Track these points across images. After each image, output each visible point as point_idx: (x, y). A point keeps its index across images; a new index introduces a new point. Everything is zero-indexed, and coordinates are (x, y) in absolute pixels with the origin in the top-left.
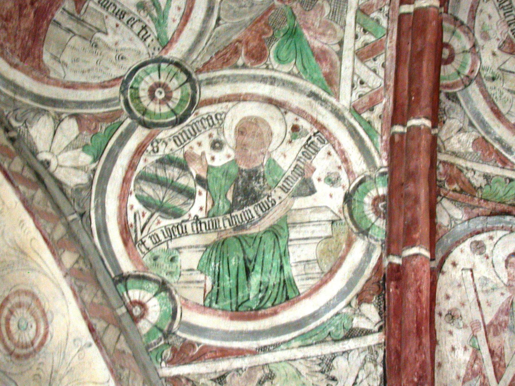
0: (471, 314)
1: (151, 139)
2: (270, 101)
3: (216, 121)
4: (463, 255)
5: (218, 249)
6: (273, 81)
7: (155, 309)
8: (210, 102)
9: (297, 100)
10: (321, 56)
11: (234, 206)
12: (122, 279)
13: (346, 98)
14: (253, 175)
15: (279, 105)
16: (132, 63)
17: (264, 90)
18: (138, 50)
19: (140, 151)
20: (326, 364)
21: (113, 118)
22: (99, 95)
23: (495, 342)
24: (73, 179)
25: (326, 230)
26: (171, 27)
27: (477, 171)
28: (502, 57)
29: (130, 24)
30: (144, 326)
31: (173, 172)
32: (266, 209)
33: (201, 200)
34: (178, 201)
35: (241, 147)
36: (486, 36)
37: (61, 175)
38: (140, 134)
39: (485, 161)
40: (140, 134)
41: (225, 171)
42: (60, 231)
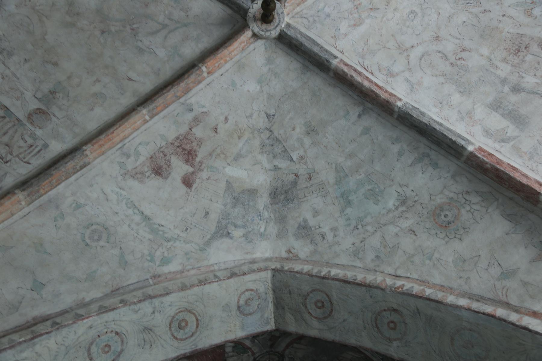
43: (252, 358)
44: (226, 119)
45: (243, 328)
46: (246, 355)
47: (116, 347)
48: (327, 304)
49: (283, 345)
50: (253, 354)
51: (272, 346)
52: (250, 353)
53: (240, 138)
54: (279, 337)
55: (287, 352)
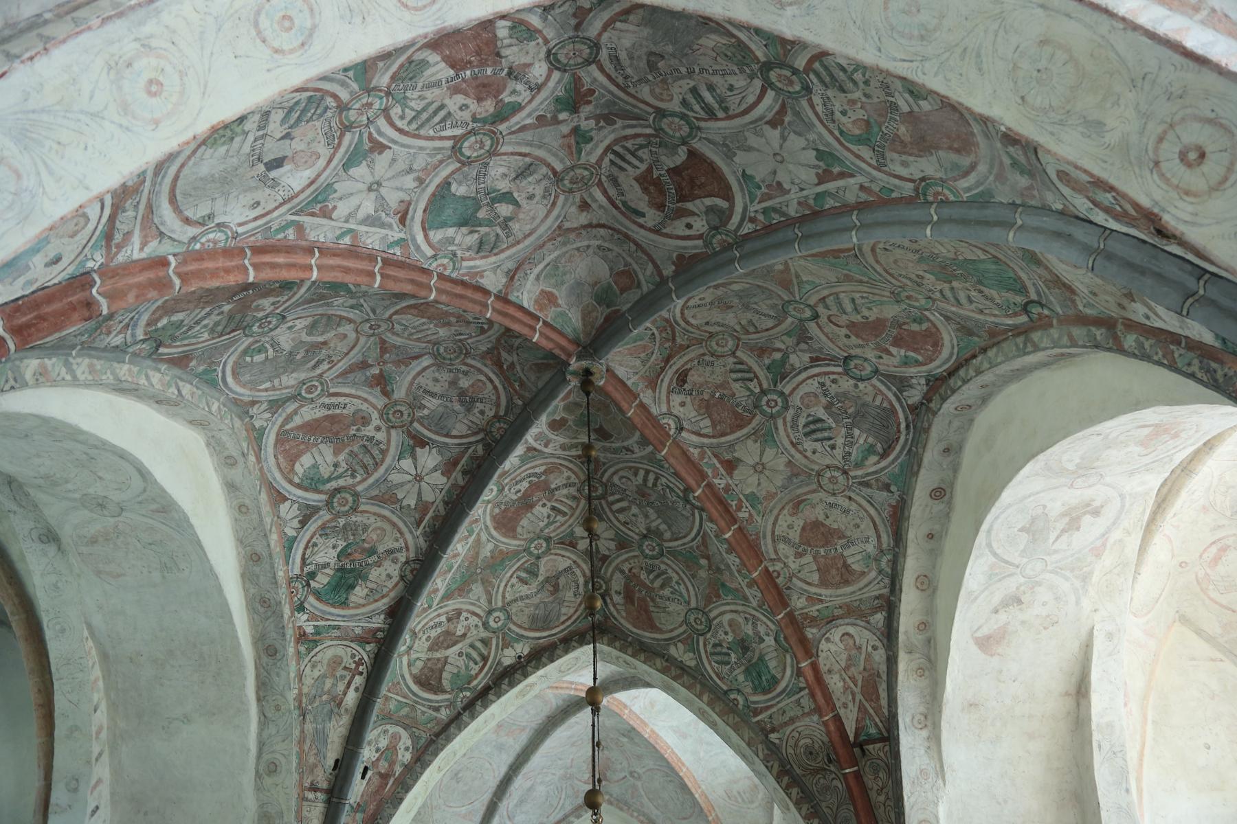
0: (836, 667)
1: (705, 640)
2: (732, 611)
3: (720, 624)
4: (824, 645)
5: (747, 672)
6: (728, 604)
7: (741, 700)
8: (715, 618)
9: (740, 608)
10: (737, 590)
11: (744, 654)
12: (726, 693)
13: (755, 603)
14: (743, 640)
15: (736, 612)
16: (683, 615)
17: (728, 608)
18: (682, 609)
19: (705, 645)
20: (798, 702)
21: (690, 636)
22: (681, 630)
23: (850, 674)
24: (693, 663)
25: (775, 654)
26: (686, 595)
27: (813, 610)
28: (798, 561)
29: (673, 600)
30: (740, 707)
31: (719, 649)
32: (754, 651)
33: (733, 655)
34: (726, 658)
35: (733, 631)
36: (787, 557)
37: (688, 663)
38: (701, 639)
39: (814, 605)
40: (701, 639)
41: (733, 642)
42: (698, 686)
43: (544, 49)
46: (533, 43)
47: (303, 20)
49: (598, 25)
50: (546, 41)
51: (577, 27)
52: (540, 40)
54: (590, 10)
55: (605, 36)
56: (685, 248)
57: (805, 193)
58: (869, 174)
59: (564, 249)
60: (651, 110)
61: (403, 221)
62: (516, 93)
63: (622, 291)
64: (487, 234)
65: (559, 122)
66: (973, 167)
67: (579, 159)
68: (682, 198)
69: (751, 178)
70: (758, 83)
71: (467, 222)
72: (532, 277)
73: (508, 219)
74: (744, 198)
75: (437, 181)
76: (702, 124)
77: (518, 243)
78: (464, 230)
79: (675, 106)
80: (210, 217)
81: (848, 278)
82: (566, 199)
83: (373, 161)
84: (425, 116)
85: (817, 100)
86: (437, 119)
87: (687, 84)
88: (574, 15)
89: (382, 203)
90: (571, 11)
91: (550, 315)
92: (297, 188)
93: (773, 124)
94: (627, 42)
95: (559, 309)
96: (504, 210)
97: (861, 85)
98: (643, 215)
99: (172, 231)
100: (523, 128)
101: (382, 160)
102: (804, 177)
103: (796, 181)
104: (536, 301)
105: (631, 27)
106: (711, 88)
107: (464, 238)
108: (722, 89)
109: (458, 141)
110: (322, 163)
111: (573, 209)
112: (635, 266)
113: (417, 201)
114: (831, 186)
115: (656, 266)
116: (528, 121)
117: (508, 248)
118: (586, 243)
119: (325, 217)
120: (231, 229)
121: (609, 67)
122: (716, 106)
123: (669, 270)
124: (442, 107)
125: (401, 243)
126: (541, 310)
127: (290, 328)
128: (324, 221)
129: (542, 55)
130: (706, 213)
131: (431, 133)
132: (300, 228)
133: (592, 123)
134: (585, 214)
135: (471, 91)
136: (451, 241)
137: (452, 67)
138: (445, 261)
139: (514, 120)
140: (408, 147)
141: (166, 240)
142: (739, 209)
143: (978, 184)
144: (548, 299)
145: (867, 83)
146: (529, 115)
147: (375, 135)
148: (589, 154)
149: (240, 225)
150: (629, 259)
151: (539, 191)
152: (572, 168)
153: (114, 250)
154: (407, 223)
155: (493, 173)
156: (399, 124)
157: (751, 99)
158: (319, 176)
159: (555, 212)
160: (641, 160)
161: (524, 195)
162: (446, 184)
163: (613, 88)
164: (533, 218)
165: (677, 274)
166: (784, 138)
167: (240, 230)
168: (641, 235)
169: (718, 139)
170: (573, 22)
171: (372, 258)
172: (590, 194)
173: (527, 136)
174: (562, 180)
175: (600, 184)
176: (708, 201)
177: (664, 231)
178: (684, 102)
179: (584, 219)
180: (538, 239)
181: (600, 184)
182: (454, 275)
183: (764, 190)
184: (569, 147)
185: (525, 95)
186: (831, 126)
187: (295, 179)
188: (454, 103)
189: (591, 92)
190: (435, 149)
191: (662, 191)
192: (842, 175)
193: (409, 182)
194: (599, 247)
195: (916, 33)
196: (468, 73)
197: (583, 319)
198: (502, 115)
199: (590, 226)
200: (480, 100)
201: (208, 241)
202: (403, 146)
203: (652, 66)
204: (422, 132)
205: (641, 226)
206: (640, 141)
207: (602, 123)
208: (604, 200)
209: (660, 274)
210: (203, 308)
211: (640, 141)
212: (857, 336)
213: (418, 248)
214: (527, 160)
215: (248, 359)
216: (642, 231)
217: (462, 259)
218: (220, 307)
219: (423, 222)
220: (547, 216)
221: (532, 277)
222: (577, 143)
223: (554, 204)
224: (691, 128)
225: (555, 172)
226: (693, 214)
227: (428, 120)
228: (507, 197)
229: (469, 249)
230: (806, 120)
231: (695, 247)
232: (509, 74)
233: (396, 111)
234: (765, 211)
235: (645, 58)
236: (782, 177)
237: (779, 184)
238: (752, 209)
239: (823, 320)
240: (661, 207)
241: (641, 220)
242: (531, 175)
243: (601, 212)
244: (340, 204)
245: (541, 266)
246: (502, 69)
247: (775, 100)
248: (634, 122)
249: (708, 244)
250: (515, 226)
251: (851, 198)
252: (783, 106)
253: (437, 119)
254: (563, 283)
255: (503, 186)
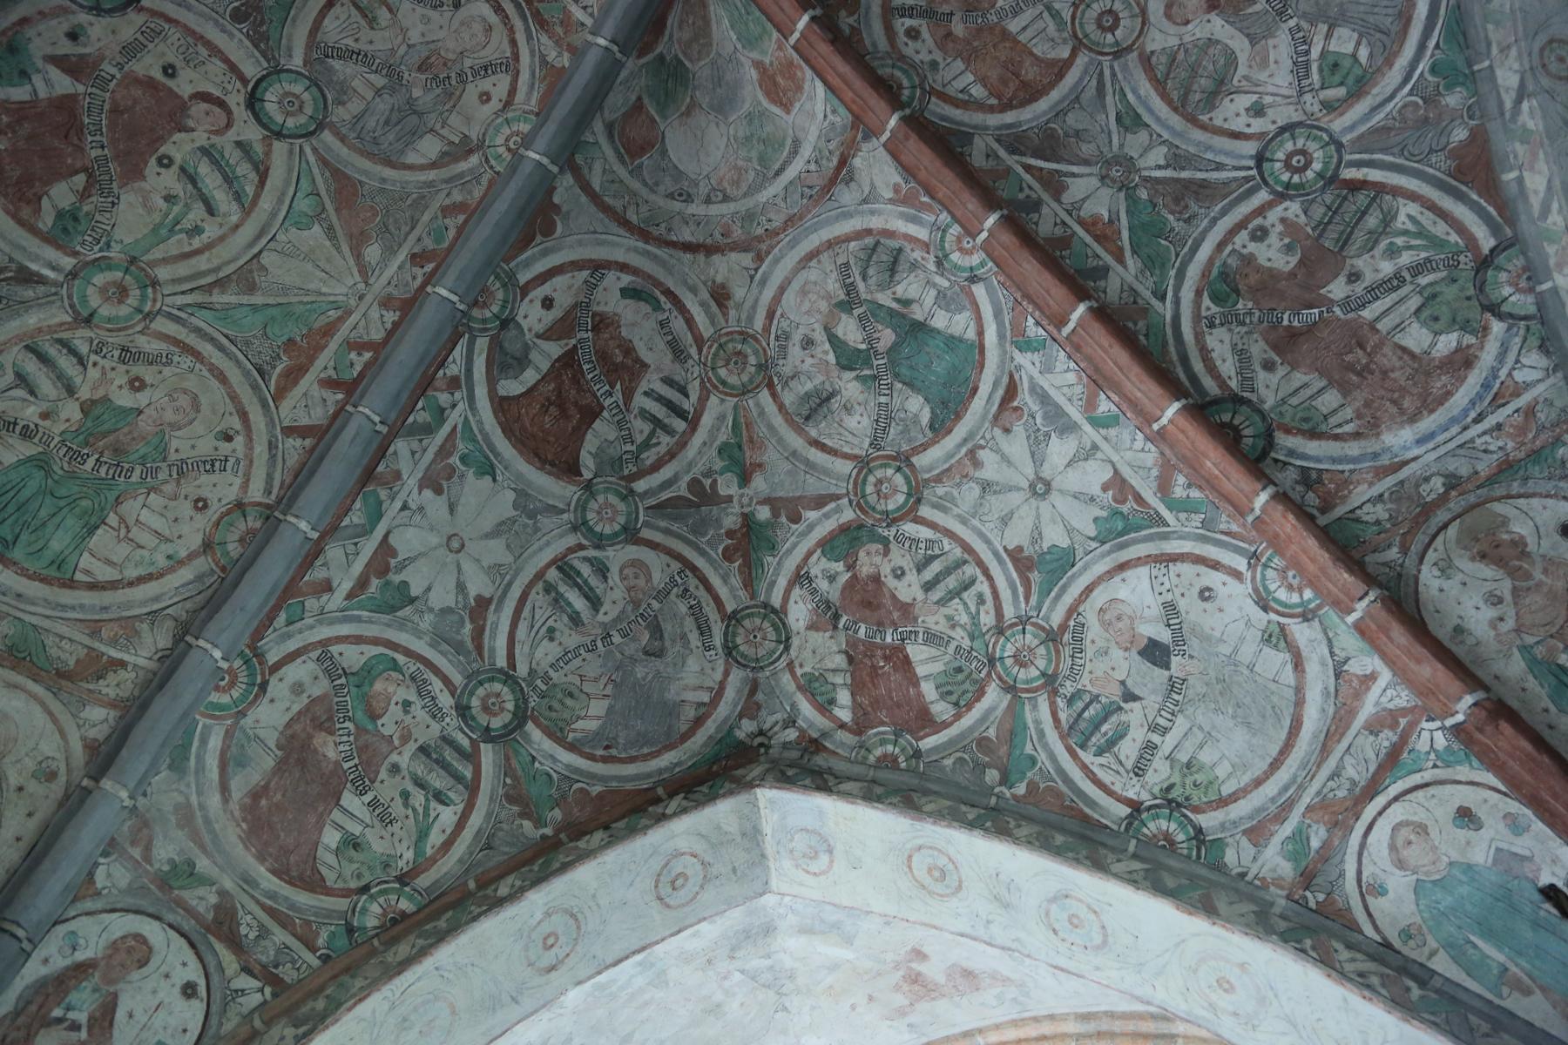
43: (793, 653)
44: (853, 1007)
45: (821, 813)
46: (807, 669)
48: (665, 890)
49: (730, 693)
50: (790, 666)
51: (754, 687)
52: (799, 672)
53: (831, 987)
55: (718, 676)
56: (545, 253)
57: (398, 504)
58: (331, 623)
59: (749, 203)
60: (646, 533)
61: (1011, 391)
62: (829, 575)
63: (638, 107)
64: (882, 287)
65: (767, 501)
66: (224, 789)
67: (735, 407)
68: (568, 361)
69: (480, 473)
70: (522, 670)
71: (914, 330)
72: (806, 151)
73: (846, 306)
74: (480, 422)
75: (950, 442)
76: (571, 540)
77: (830, 245)
78: (919, 315)
79: (616, 556)
80: (1267, 639)
81: (246, 277)
82: (750, 318)
83: (1034, 542)
84: (951, 582)
85: (445, 700)
86: (936, 567)
87: (609, 612)
88: (759, 707)
89: (1037, 445)
90: (763, 713)
91: (772, 49)
92: (1143, 571)
93: (483, 603)
94: (693, 664)
95: (755, 55)
96: (850, 331)
97: (410, 787)
98: (626, 293)
99: (1323, 664)
100: (820, 502)
101: (1017, 535)
102: (410, 533)
103: (417, 518)
104: (799, 88)
105: (691, 696)
106: (576, 620)
107: (918, 290)
108: (561, 623)
109: (910, 512)
110: (1099, 597)
111: (739, 293)
112: (622, 172)
113: (984, 417)
114: (369, 547)
115: (586, 187)
116: (811, 515)
117: (847, 239)
118: (715, 210)
119: (1124, 481)
120: (1253, 579)
121: (710, 610)
122: (562, 588)
123: (565, 190)
124: (928, 587)
125: (1026, 345)
126: (791, 64)
127: (1258, 111)
128: (1126, 472)
129: (795, 642)
130: (527, 349)
131: (947, 544)
132: (1164, 488)
133: (723, 491)
134: (719, 279)
135: (888, 602)
136: (942, 299)
137: (907, 661)
138: (955, 257)
139: (830, 525)
140: (981, 535)
141: (1342, 655)
142: (481, 392)
143: (201, 768)
144: (780, 89)
145: (405, 795)
146: (811, 527)
147: (1021, 590)
148: (721, 418)
149: (1237, 575)
150: (636, 185)
151: (795, 351)
152: (745, 391)
153: (1403, 722)
154: (1005, 380)
155: (866, 421)
156: (983, 587)
157: (522, 632)
158: (1110, 574)
159: (768, 294)
160: (645, 415)
161: (818, 351)
162: (939, 428)
163: (700, 562)
164: (804, 292)
165: (551, 190)
166: (461, 587)
167: (1241, 564)
168: (623, 248)
169: (546, 522)
170: (760, 697)
171: (1074, 347)
172: (713, 323)
173: (814, 486)
174: (759, 366)
175: (699, 341)
176: (530, 377)
177: (585, 273)
178: (602, 570)
179: (725, 267)
180: (793, 244)
181: (699, 341)
182: (944, 217)
183: (455, 460)
184: (751, 441)
185: (819, 566)
186: (413, 667)
187: (1138, 593)
188: (908, 589)
189: (728, 556)
190: (944, 510)
191: (603, 357)
192: (362, 584)
193: (991, 468)
194: (689, 199)
195: (412, 1018)
196: (889, 639)
197: (706, 20)
198: (844, 542)
199: (710, 250)
200: (876, 579)
201: (1290, 588)
202: (988, 542)
203: (657, 631)
204: (959, 552)
205: (624, 267)
206: (650, 457)
207: (707, 482)
208: (689, 305)
209: (576, 170)
210: (1372, 326)
211: (650, 457)
212: (150, 84)
213: (998, 314)
214: (813, 433)
215: (1363, 54)
216: (619, 256)
217: (926, 246)
218: (1346, 304)
219: (982, 366)
220: (782, 290)
221: (806, 151)
222: (740, 447)
223: (771, 315)
224: (585, 523)
225: (771, 386)
226: (546, 335)
227: (948, 571)
228: (849, 359)
229: (914, 266)
230: (445, 647)
231: (527, 264)
232: (836, 617)
233: (987, 619)
234: (441, 414)
235: (667, 643)
236: (435, 505)
237: (438, 491)
238: (461, 406)
239: (236, 100)
240: (602, 323)
241: (626, 279)
242: (808, 395)
243: (693, 279)
244: (1096, 490)
245: (791, 172)
246: (846, 629)
247: (492, 650)
248: (665, 496)
249: (509, 281)
250: (833, 286)
251: (334, 552)
252: (479, 648)
253: (936, 567)
254: (750, 117)
255: (850, 387)
